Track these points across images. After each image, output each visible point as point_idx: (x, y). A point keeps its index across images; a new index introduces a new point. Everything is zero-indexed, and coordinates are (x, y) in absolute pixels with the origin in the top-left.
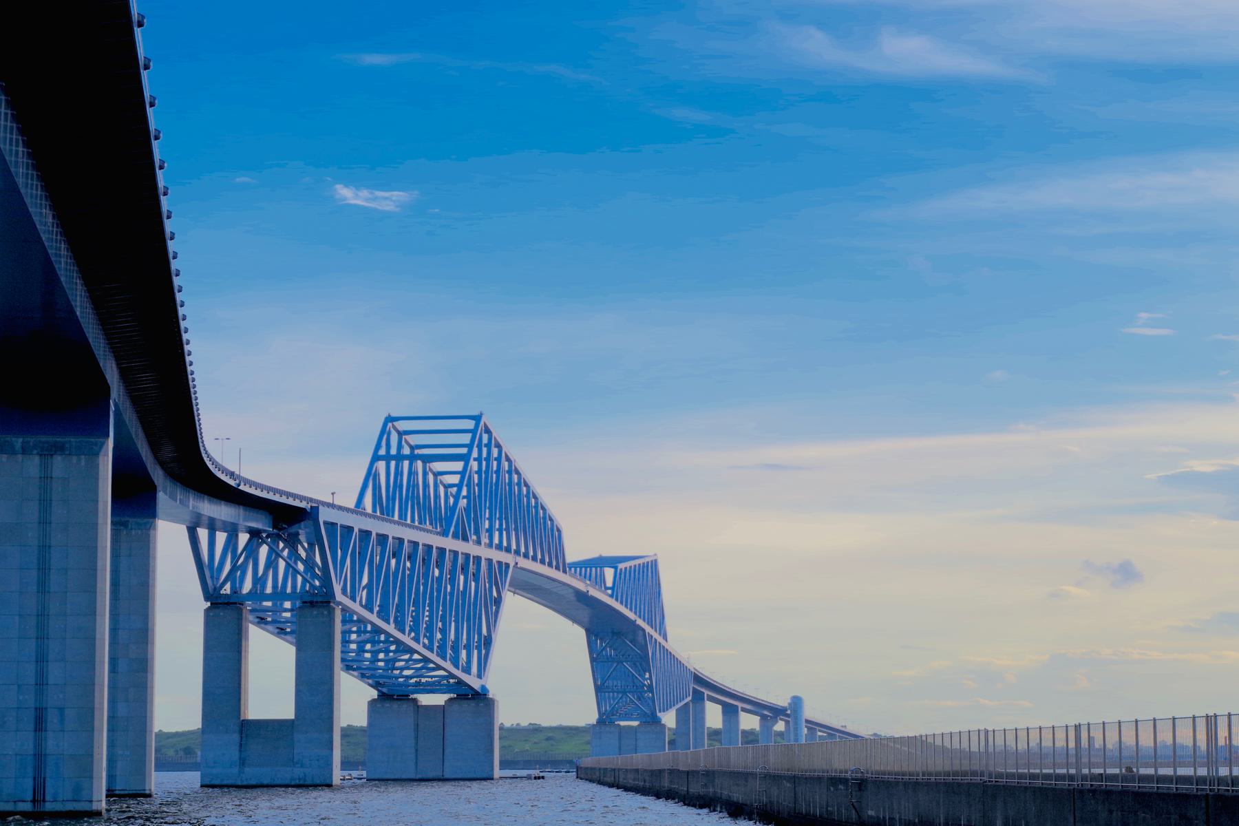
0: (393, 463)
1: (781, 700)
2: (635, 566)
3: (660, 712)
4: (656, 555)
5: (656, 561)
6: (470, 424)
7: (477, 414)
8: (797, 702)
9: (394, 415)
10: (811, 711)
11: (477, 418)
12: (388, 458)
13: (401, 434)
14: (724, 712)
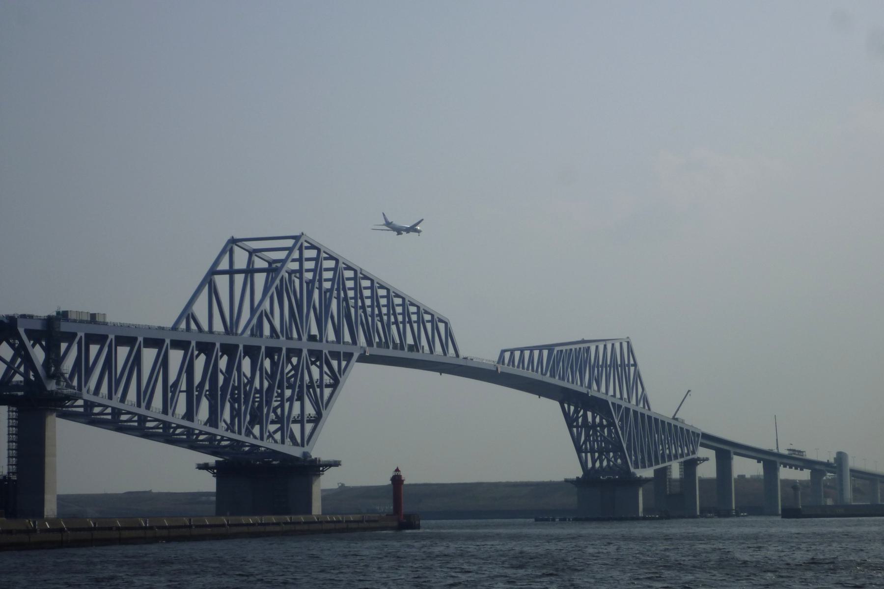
0: (239, 279)
1: (826, 455)
2: (580, 348)
3: (637, 467)
4: (628, 338)
5: (628, 343)
6: (290, 243)
7: (298, 234)
8: (841, 457)
9: (237, 237)
10: (855, 462)
11: (296, 238)
12: (231, 272)
13: (252, 253)
14: (765, 468)
